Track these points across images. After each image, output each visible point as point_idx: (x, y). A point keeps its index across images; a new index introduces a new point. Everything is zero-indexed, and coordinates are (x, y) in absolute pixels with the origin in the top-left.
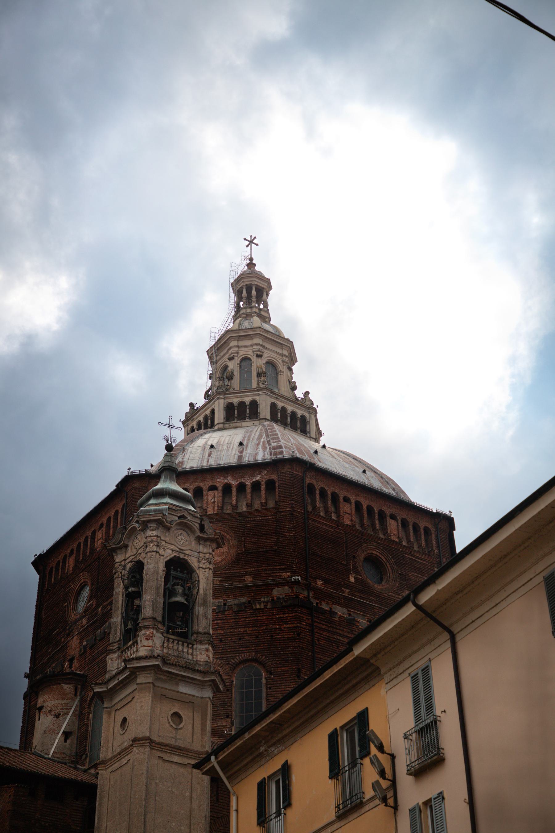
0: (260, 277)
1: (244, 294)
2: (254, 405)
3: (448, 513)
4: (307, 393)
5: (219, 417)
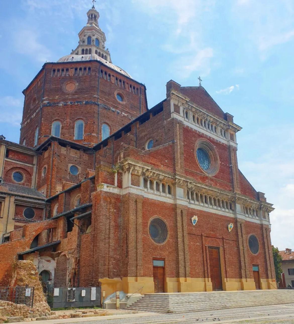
0: (96, 11)
1: (90, 17)
2: (90, 50)
3: (144, 84)
4: (108, 49)
5: (80, 52)
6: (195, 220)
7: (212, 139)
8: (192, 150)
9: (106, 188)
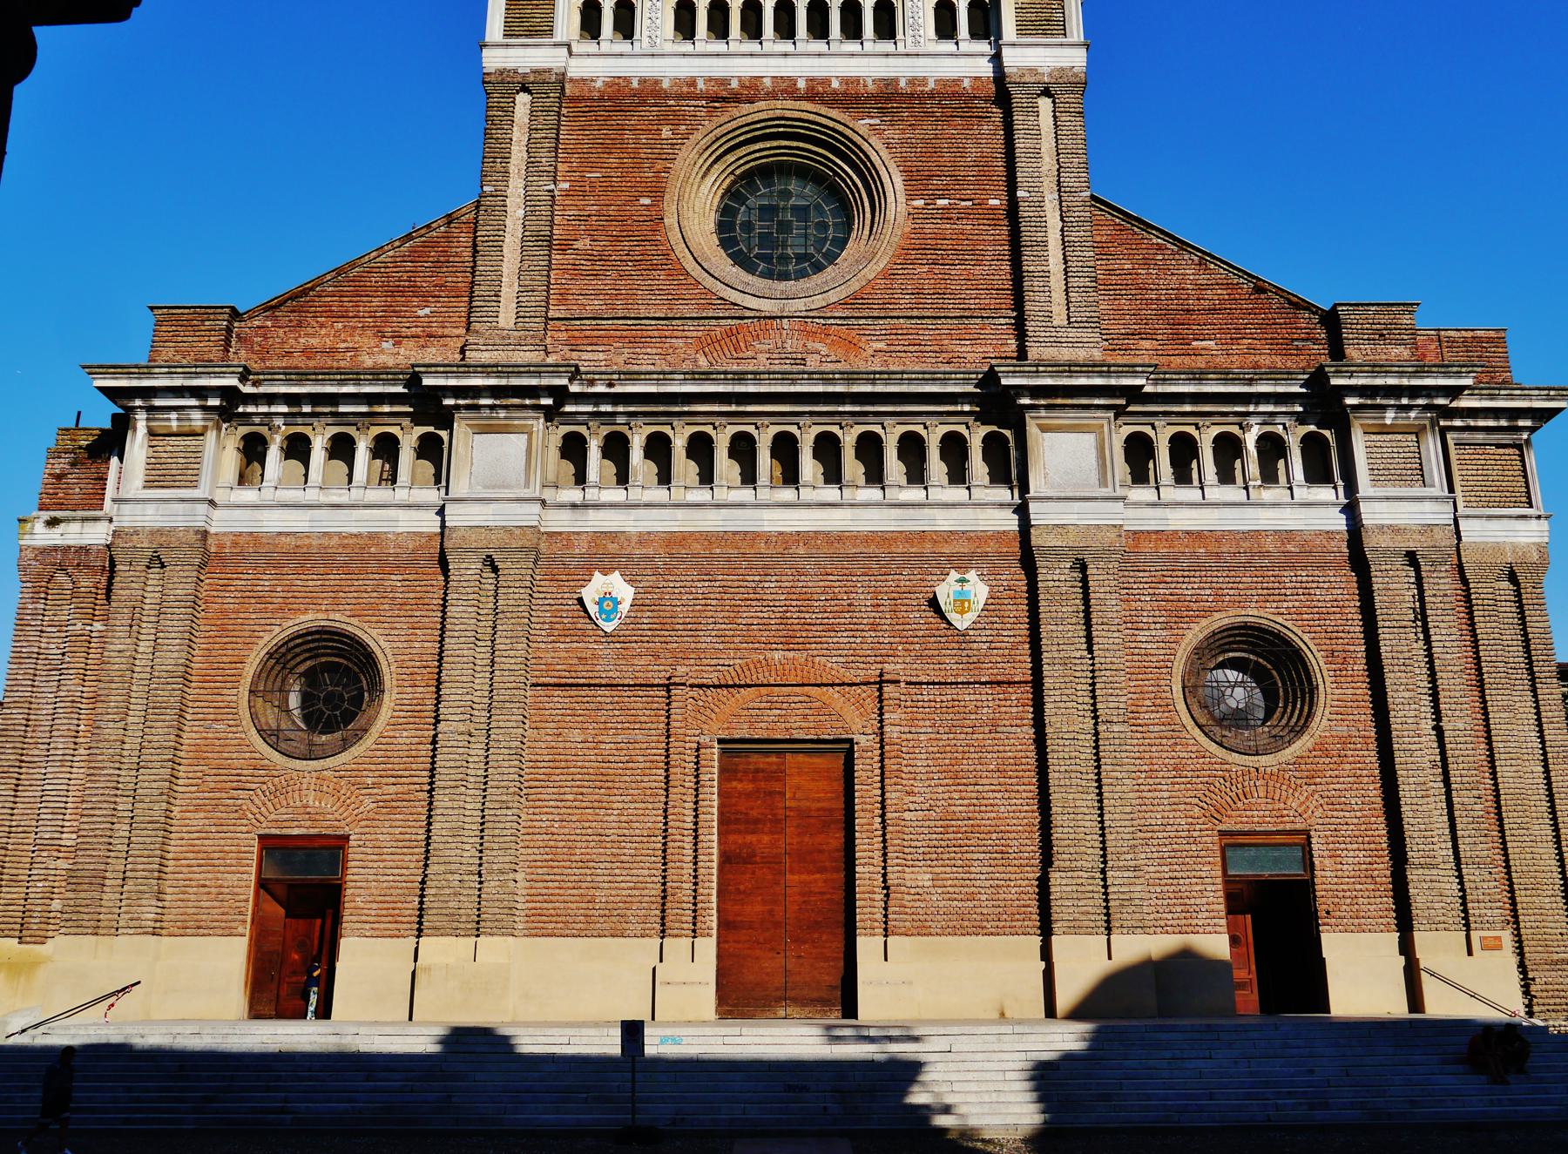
6: (607, 599)
7: (835, 84)
8: (647, 201)
9: (45, 530)
